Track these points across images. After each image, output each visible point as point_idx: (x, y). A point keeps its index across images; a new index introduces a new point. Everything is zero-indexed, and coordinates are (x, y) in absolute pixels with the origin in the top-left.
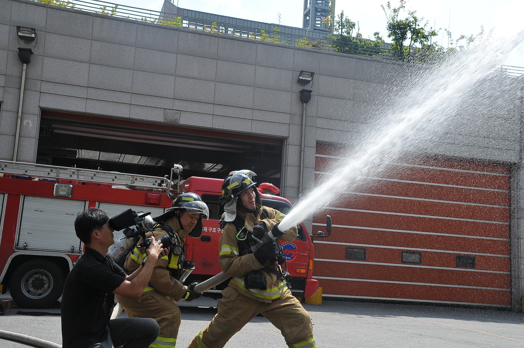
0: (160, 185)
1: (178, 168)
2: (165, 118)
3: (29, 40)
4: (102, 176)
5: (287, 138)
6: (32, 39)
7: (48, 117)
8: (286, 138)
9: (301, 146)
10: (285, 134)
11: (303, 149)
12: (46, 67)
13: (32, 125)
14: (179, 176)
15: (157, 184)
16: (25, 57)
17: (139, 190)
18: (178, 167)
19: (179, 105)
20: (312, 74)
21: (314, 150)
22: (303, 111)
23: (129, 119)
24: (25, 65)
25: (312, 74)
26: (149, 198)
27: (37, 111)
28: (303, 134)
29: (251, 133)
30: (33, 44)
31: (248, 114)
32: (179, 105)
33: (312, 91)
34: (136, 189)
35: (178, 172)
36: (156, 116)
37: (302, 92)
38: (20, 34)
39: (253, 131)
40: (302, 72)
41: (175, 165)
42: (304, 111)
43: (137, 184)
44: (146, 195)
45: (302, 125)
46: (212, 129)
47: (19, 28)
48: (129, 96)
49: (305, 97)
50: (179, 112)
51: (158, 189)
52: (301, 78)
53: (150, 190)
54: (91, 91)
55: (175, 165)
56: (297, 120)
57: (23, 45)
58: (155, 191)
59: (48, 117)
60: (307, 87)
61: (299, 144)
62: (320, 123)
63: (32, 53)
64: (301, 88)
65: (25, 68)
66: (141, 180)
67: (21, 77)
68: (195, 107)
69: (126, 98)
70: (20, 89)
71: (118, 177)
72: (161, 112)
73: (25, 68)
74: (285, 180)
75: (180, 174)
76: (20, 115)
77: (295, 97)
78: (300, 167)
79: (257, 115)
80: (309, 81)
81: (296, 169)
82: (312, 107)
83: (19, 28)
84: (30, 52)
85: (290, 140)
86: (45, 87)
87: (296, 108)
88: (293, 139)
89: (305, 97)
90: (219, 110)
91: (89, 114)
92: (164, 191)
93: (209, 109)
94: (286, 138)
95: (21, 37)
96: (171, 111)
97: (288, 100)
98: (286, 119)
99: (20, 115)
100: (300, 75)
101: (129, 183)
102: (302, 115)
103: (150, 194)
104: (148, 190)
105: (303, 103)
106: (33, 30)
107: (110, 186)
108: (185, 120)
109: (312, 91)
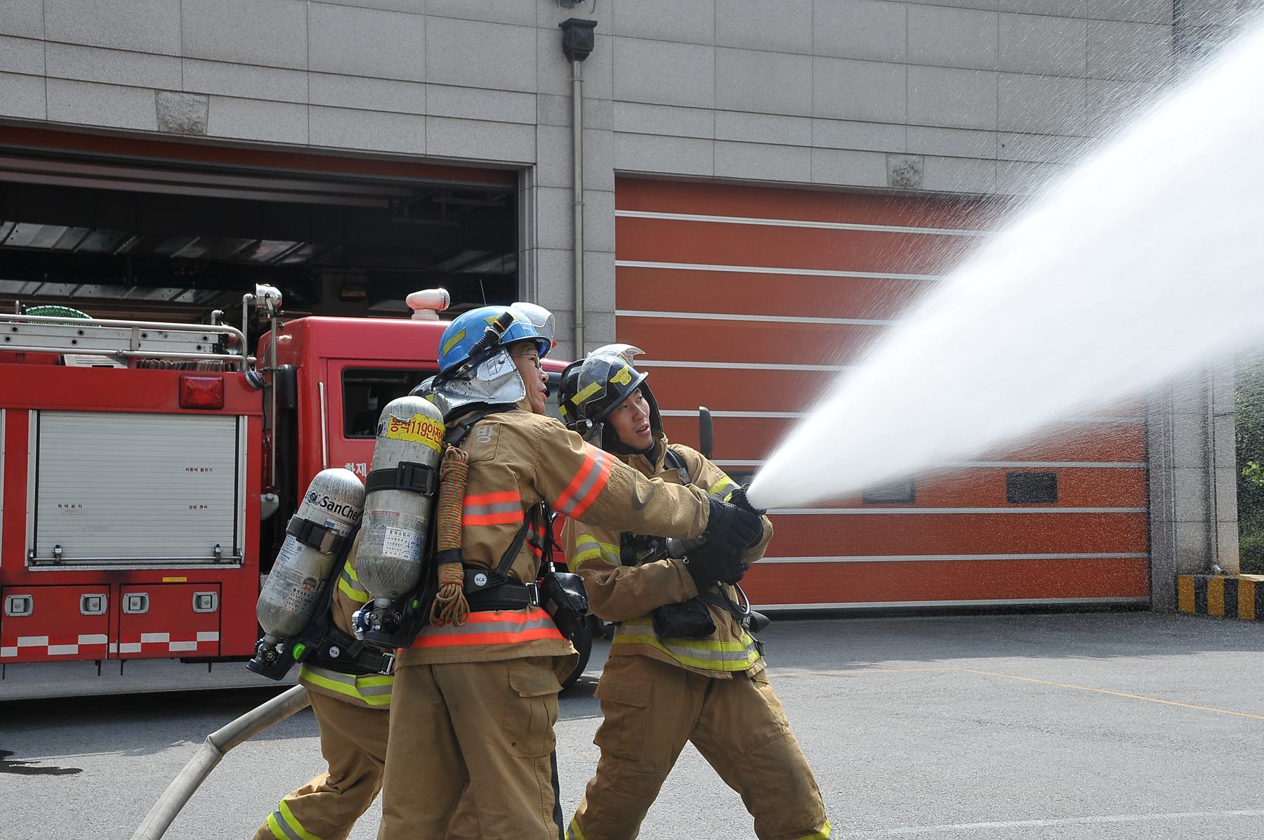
0: (218, 348)
2: (162, 120)
4: (37, 331)
5: (530, 168)
8: (529, 168)
9: (573, 188)
11: (578, 199)
15: (208, 347)
17: (156, 366)
19: (199, 77)
22: (572, 84)
23: (46, 123)
28: (577, 154)
31: (412, 98)
32: (199, 77)
33: (594, 24)
35: (271, 308)
41: (258, 287)
42: (577, 84)
43: (153, 348)
44: (181, 381)
45: (572, 126)
48: (38, 49)
49: (576, 42)
50: (203, 99)
53: (190, 365)
56: (558, 112)
58: (203, 366)
60: (581, 13)
61: (566, 183)
62: (625, 117)
64: (565, 15)
66: (160, 337)
68: (250, 82)
72: (148, 100)
75: (275, 315)
77: (548, 41)
78: (573, 250)
79: (440, 101)
81: (563, 258)
87: (553, 74)
88: (549, 172)
89: (576, 42)
90: (324, 91)
92: (231, 365)
93: (295, 86)
94: (529, 168)
96: (177, 97)
97: (529, 52)
98: (524, 109)
101: (124, 349)
104: (184, 367)
107: (58, 359)
109: (594, 24)
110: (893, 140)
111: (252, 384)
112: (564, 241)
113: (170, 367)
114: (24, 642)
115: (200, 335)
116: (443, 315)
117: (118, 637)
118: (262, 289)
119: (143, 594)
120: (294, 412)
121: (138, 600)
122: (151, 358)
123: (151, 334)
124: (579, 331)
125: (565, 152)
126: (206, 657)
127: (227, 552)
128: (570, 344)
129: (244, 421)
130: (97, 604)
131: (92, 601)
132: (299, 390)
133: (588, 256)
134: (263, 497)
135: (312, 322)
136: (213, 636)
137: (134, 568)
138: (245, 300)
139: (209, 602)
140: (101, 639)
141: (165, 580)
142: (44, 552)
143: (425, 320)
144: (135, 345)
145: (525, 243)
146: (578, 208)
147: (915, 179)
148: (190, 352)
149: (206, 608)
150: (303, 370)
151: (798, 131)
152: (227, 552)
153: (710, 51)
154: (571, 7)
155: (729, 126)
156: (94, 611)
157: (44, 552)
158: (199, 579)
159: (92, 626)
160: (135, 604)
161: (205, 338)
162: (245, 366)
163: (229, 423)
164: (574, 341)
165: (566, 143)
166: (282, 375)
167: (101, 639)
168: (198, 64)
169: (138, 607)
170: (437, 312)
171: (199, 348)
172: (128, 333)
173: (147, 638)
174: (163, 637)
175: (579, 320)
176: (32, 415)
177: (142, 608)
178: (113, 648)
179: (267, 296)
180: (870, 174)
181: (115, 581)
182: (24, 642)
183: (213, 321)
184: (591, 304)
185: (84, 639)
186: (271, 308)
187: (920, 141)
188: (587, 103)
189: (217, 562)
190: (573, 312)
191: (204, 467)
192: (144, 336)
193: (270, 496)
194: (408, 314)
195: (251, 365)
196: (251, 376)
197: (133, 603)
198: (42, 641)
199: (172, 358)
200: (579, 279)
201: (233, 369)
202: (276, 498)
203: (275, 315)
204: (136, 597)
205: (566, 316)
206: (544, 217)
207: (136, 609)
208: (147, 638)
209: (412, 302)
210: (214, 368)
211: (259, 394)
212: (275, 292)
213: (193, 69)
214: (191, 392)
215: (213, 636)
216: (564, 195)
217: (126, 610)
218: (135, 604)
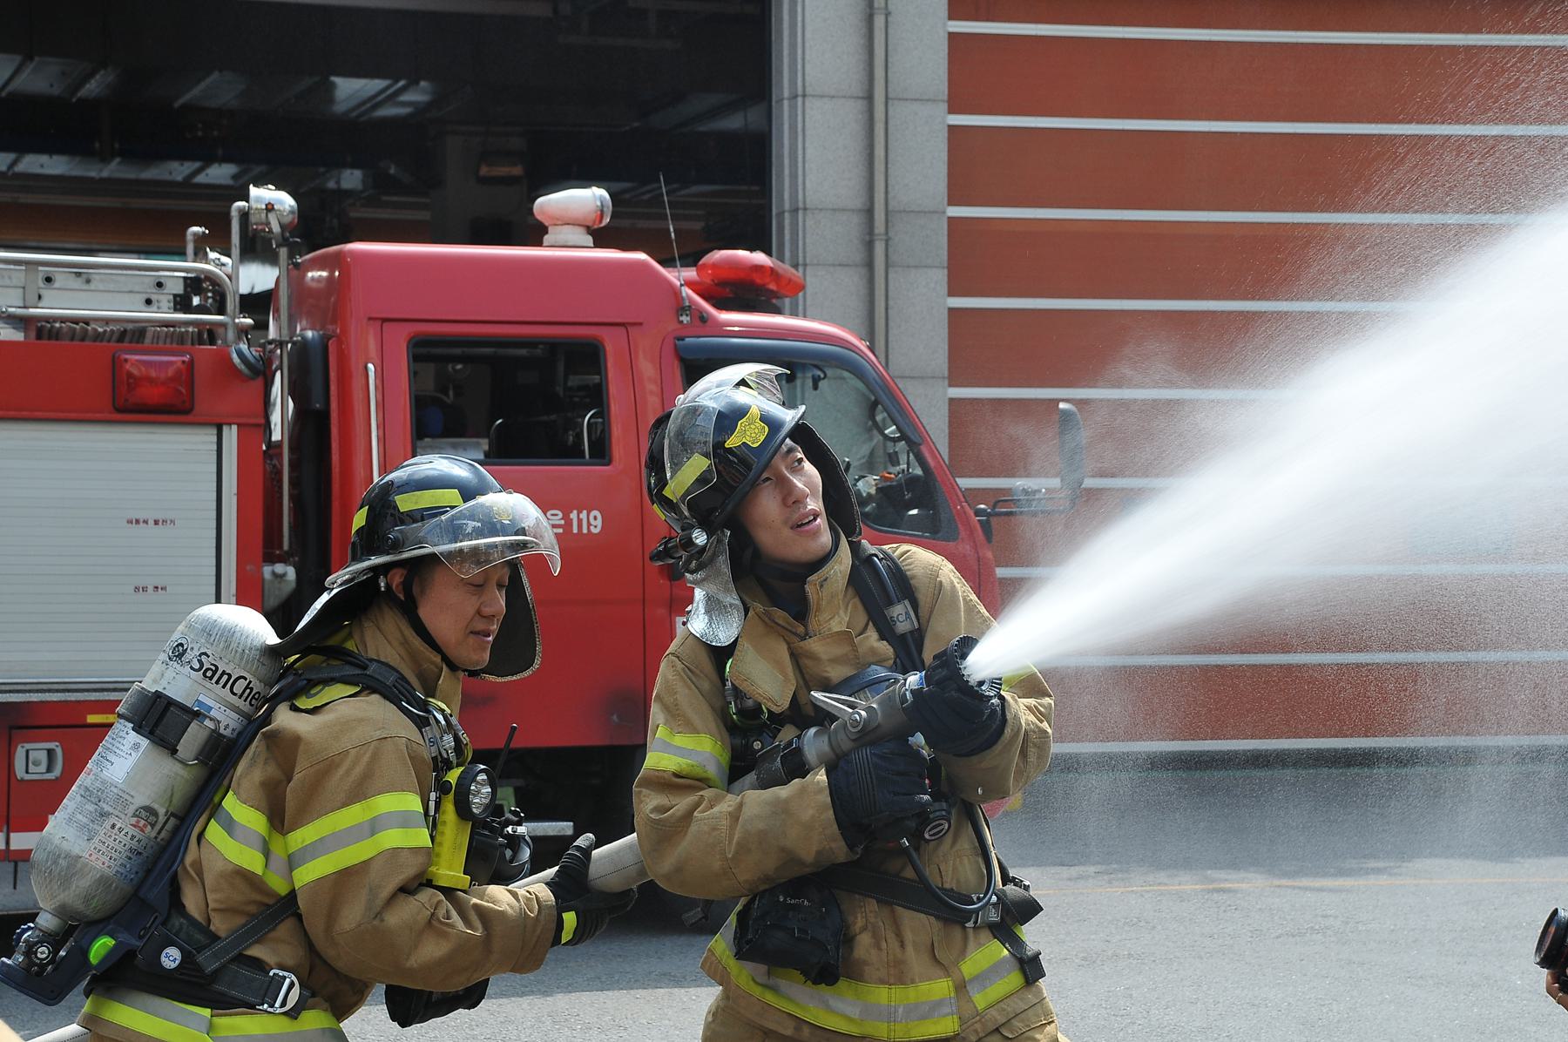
0: (182, 303)
14: (283, 252)
15: (165, 300)
17: (73, 335)
18: (272, 200)
26: (130, 375)
34: (55, 335)
35: (276, 228)
43: (59, 305)
44: (116, 364)
53: (133, 334)
58: (157, 336)
66: (78, 283)
74: (794, 176)
75: (284, 242)
78: (869, 98)
81: (851, 113)
103: (134, 360)
111: (242, 367)
113: (98, 337)
116: (601, 237)
118: (261, 194)
119: (52, 745)
120: (324, 415)
121: (43, 756)
122: (63, 320)
124: (879, 248)
128: (863, 271)
129: (231, 435)
132: (333, 375)
133: (899, 112)
134: (267, 570)
135: (352, 252)
137: (35, 697)
138: (234, 214)
141: (92, 719)
143: (567, 247)
144: (32, 298)
145: (783, 86)
146: (879, 21)
148: (131, 310)
150: (340, 342)
160: (37, 764)
161: (160, 285)
162: (231, 335)
163: (207, 437)
164: (870, 264)
166: (302, 348)
169: (43, 768)
170: (590, 231)
171: (149, 302)
172: (19, 275)
175: (879, 226)
177: (49, 770)
179: (270, 208)
183: (190, 248)
186: (276, 228)
190: (869, 212)
191: (160, 517)
192: (48, 280)
193: (279, 568)
194: (534, 233)
195: (243, 332)
196: (240, 354)
199: (107, 321)
201: (212, 341)
202: (291, 573)
203: (284, 242)
204: (38, 750)
205: (855, 222)
207: (38, 772)
209: (543, 213)
210: (173, 337)
211: (259, 382)
212: (285, 201)
214: (134, 382)
217: (20, 772)
218: (37, 764)
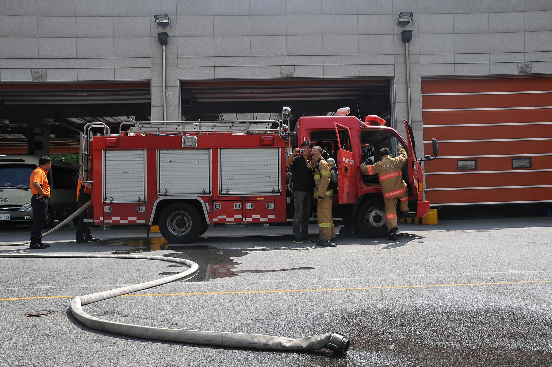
0: (272, 127)
1: (286, 110)
2: (282, 74)
3: (165, 25)
6: (167, 24)
7: (187, 87)
9: (407, 83)
10: (392, 75)
11: (409, 86)
12: (180, 45)
13: (175, 96)
15: (269, 127)
16: (163, 39)
19: (292, 61)
20: (411, 14)
21: (420, 85)
23: (251, 79)
24: (164, 46)
25: (411, 14)
27: (177, 84)
29: (359, 78)
30: (168, 28)
32: (292, 61)
33: (412, 31)
36: (274, 74)
37: (403, 33)
38: (157, 21)
39: (362, 75)
40: (401, 14)
41: (283, 108)
42: (407, 50)
43: (251, 129)
44: (261, 138)
45: (406, 64)
46: (324, 78)
47: (156, 17)
48: (249, 59)
49: (406, 37)
51: (272, 131)
52: (401, 20)
54: (217, 59)
55: (283, 108)
56: (401, 59)
57: (162, 30)
59: (187, 87)
60: (408, 28)
61: (404, 81)
62: (423, 59)
63: (168, 36)
64: (402, 29)
65: (164, 49)
67: (162, 57)
69: (246, 61)
70: (162, 67)
71: (234, 125)
73: (164, 49)
76: (164, 89)
77: (397, 38)
78: (407, 102)
80: (408, 22)
81: (404, 105)
82: (414, 45)
83: (156, 17)
84: (166, 35)
85: (396, 79)
86: (181, 62)
87: (399, 48)
88: (399, 78)
89: (406, 37)
90: (328, 61)
91: (217, 80)
95: (158, 24)
96: (286, 67)
97: (391, 42)
99: (164, 89)
100: (400, 18)
101: (245, 129)
102: (406, 55)
105: (405, 43)
106: (167, 16)
108: (300, 74)
109: (412, 31)
110: (520, 58)
112: (404, 99)
114: (219, 217)
115: (267, 124)
117: (246, 217)
123: (252, 124)
125: (404, 72)
126: (273, 224)
127: (277, 191)
129: (280, 149)
130: (239, 206)
131: (238, 205)
133: (413, 104)
136: (273, 216)
139: (271, 206)
140: (240, 217)
142: (224, 191)
146: (409, 89)
147: (528, 70)
149: (270, 208)
151: (485, 58)
152: (277, 191)
153: (452, 35)
154: (404, 27)
155: (460, 59)
156: (238, 208)
157: (224, 191)
158: (268, 199)
159: (238, 212)
165: (404, 69)
167: (240, 217)
168: (291, 57)
172: (246, 124)
173: (254, 217)
174: (258, 217)
176: (219, 150)
178: (244, 219)
180: (512, 70)
181: (244, 199)
182: (219, 217)
184: (414, 119)
185: (236, 217)
187: (530, 57)
188: (410, 56)
189: (273, 193)
197: (249, 206)
198: (224, 217)
200: (410, 111)
204: (250, 204)
206: (398, 93)
207: (250, 208)
208: (254, 217)
212: (289, 109)
213: (290, 59)
215: (273, 216)
216: (404, 85)
